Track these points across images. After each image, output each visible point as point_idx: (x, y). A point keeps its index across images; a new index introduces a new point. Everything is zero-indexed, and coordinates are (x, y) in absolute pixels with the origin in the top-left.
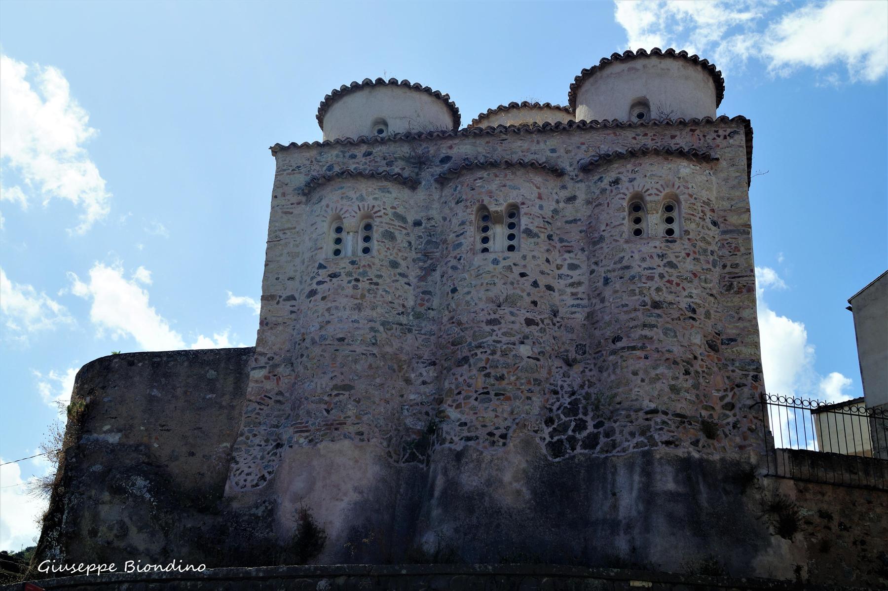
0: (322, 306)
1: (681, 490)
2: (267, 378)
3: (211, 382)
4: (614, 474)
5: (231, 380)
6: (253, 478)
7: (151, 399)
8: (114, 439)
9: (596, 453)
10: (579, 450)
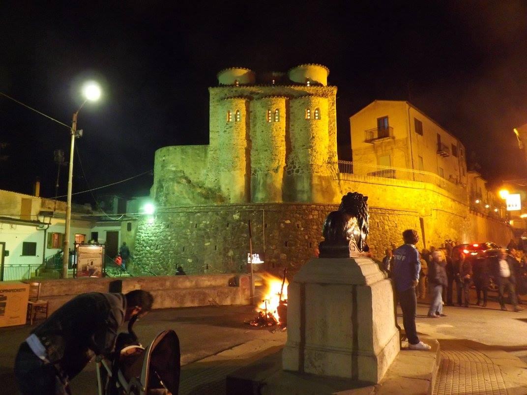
0: (228, 135)
1: (319, 183)
2: (214, 153)
3: (198, 154)
4: (303, 179)
5: (204, 154)
6: (213, 180)
7: (182, 159)
8: (174, 169)
9: (299, 174)
10: (294, 173)
